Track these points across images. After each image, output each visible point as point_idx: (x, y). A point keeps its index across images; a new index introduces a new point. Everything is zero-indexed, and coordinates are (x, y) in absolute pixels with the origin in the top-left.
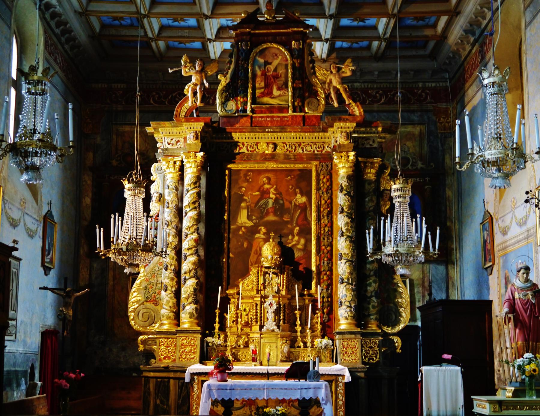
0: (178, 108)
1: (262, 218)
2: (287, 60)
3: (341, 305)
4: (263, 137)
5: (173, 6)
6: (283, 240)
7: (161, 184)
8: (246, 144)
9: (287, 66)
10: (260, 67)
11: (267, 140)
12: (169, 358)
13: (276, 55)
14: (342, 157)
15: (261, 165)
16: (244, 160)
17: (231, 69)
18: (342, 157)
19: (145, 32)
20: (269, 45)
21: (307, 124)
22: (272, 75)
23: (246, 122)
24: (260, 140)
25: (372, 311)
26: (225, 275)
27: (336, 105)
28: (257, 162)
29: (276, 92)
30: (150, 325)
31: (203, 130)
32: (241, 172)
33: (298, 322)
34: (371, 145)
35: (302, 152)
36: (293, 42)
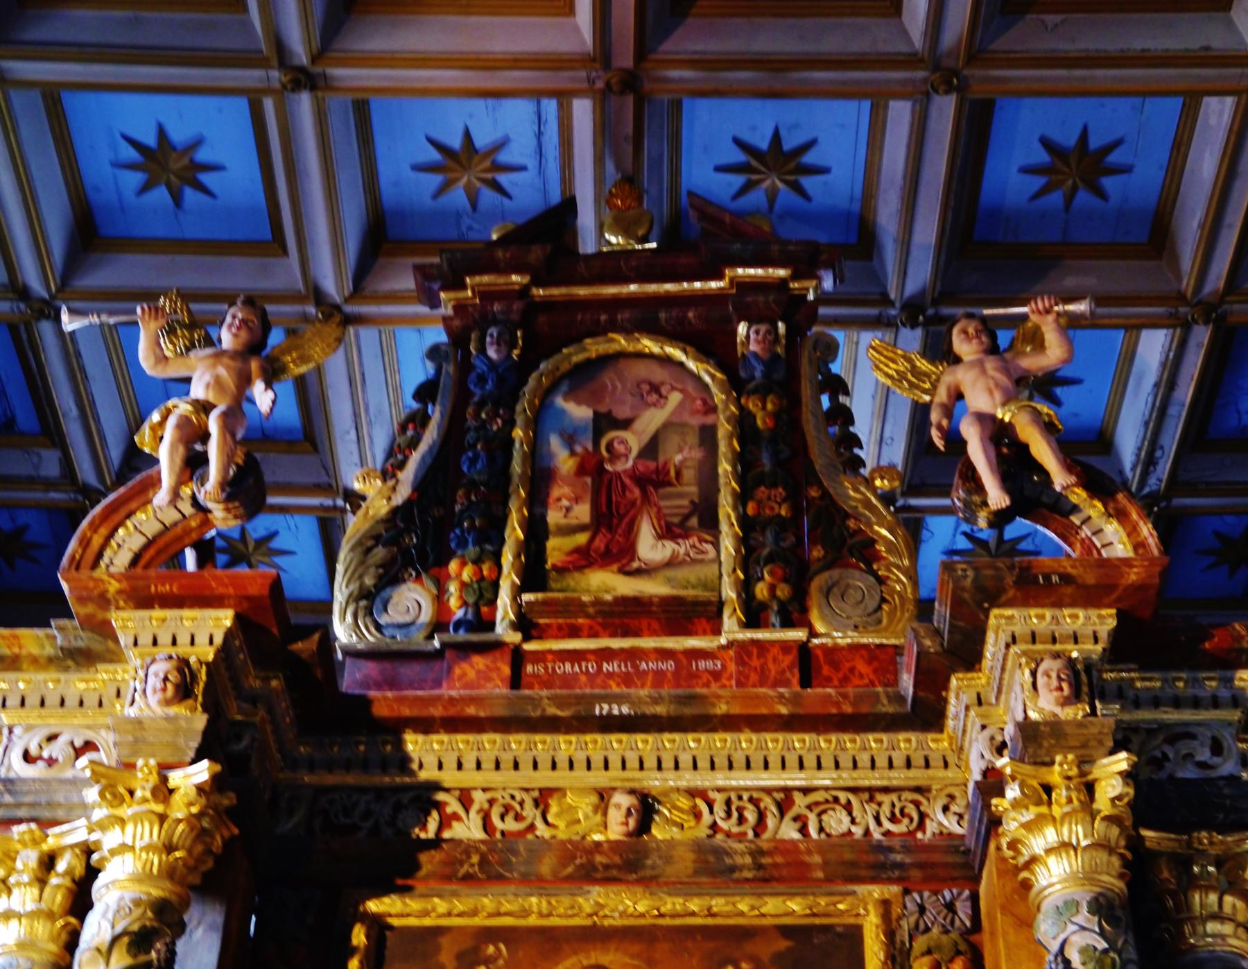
0: (94, 527)
2: (711, 409)
4: (580, 757)
5: (182, 259)
8: (479, 798)
9: (708, 436)
10: (570, 440)
11: (599, 778)
14: (1048, 789)
15: (562, 903)
16: (468, 879)
17: (423, 447)
18: (1048, 789)
19: (67, 463)
20: (621, 342)
21: (827, 696)
22: (635, 476)
23: (484, 676)
24: (560, 778)
29: (649, 547)
31: (225, 651)
32: (444, 941)
34: (1203, 765)
35: (796, 836)
36: (742, 328)
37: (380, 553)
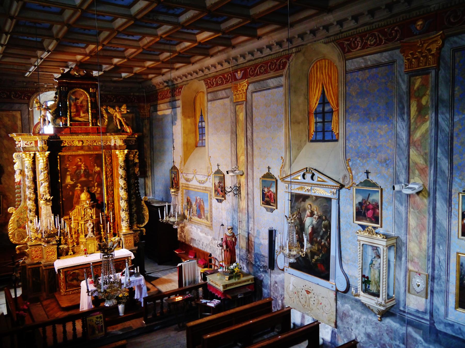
1: (78, 179)
2: (88, 98)
3: (123, 220)
6: (90, 189)
7: (20, 165)
9: (87, 101)
10: (73, 101)
12: (38, 257)
13: (81, 95)
20: (78, 89)
25: (135, 220)
26: (61, 210)
27: (119, 128)
28: (74, 151)
29: (82, 115)
30: (22, 240)
33: (102, 230)
37: (54, 115)
